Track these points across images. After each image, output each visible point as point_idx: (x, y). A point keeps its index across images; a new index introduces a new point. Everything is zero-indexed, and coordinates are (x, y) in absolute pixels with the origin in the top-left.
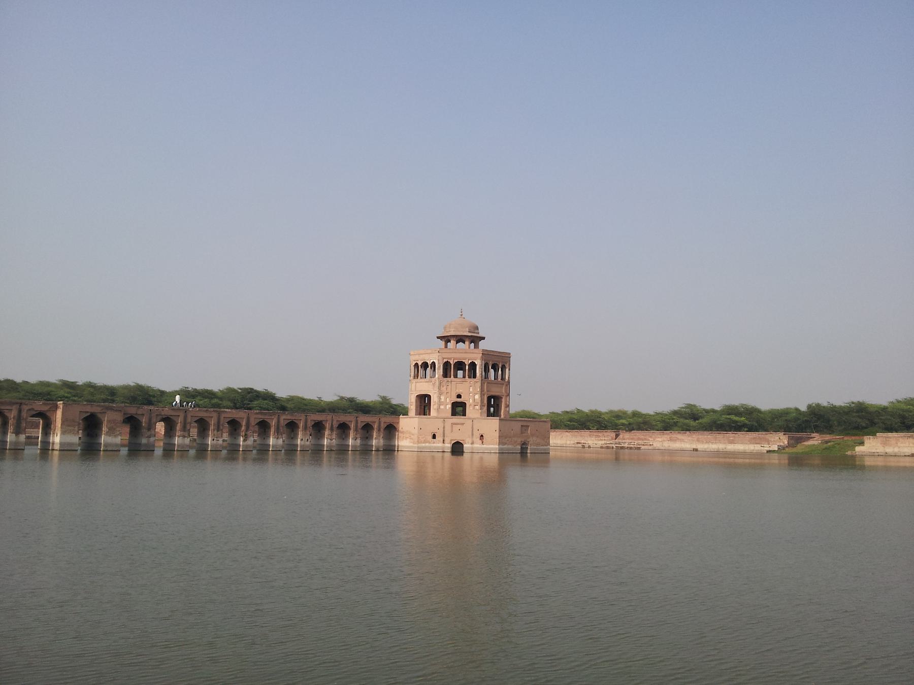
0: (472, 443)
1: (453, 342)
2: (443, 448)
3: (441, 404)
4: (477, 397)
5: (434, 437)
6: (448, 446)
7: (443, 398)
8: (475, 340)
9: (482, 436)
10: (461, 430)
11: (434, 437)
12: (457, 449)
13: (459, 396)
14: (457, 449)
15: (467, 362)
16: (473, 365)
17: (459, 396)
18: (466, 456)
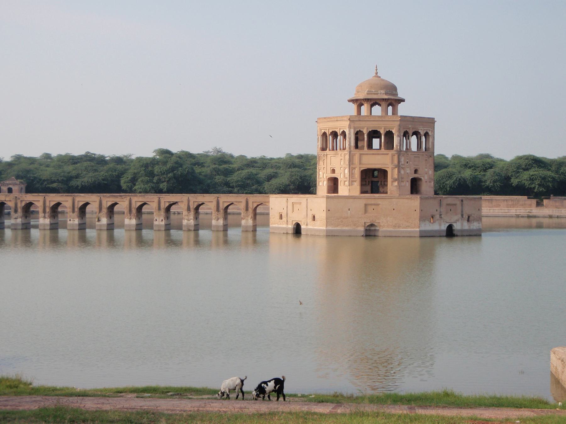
0: (307, 225)
1: (364, 109)
2: (287, 229)
4: (347, 171)
5: (281, 217)
6: (291, 226)
8: (393, 101)
9: (314, 217)
11: (281, 217)
12: (297, 230)
14: (297, 230)
17: (333, 171)
18: (303, 237)
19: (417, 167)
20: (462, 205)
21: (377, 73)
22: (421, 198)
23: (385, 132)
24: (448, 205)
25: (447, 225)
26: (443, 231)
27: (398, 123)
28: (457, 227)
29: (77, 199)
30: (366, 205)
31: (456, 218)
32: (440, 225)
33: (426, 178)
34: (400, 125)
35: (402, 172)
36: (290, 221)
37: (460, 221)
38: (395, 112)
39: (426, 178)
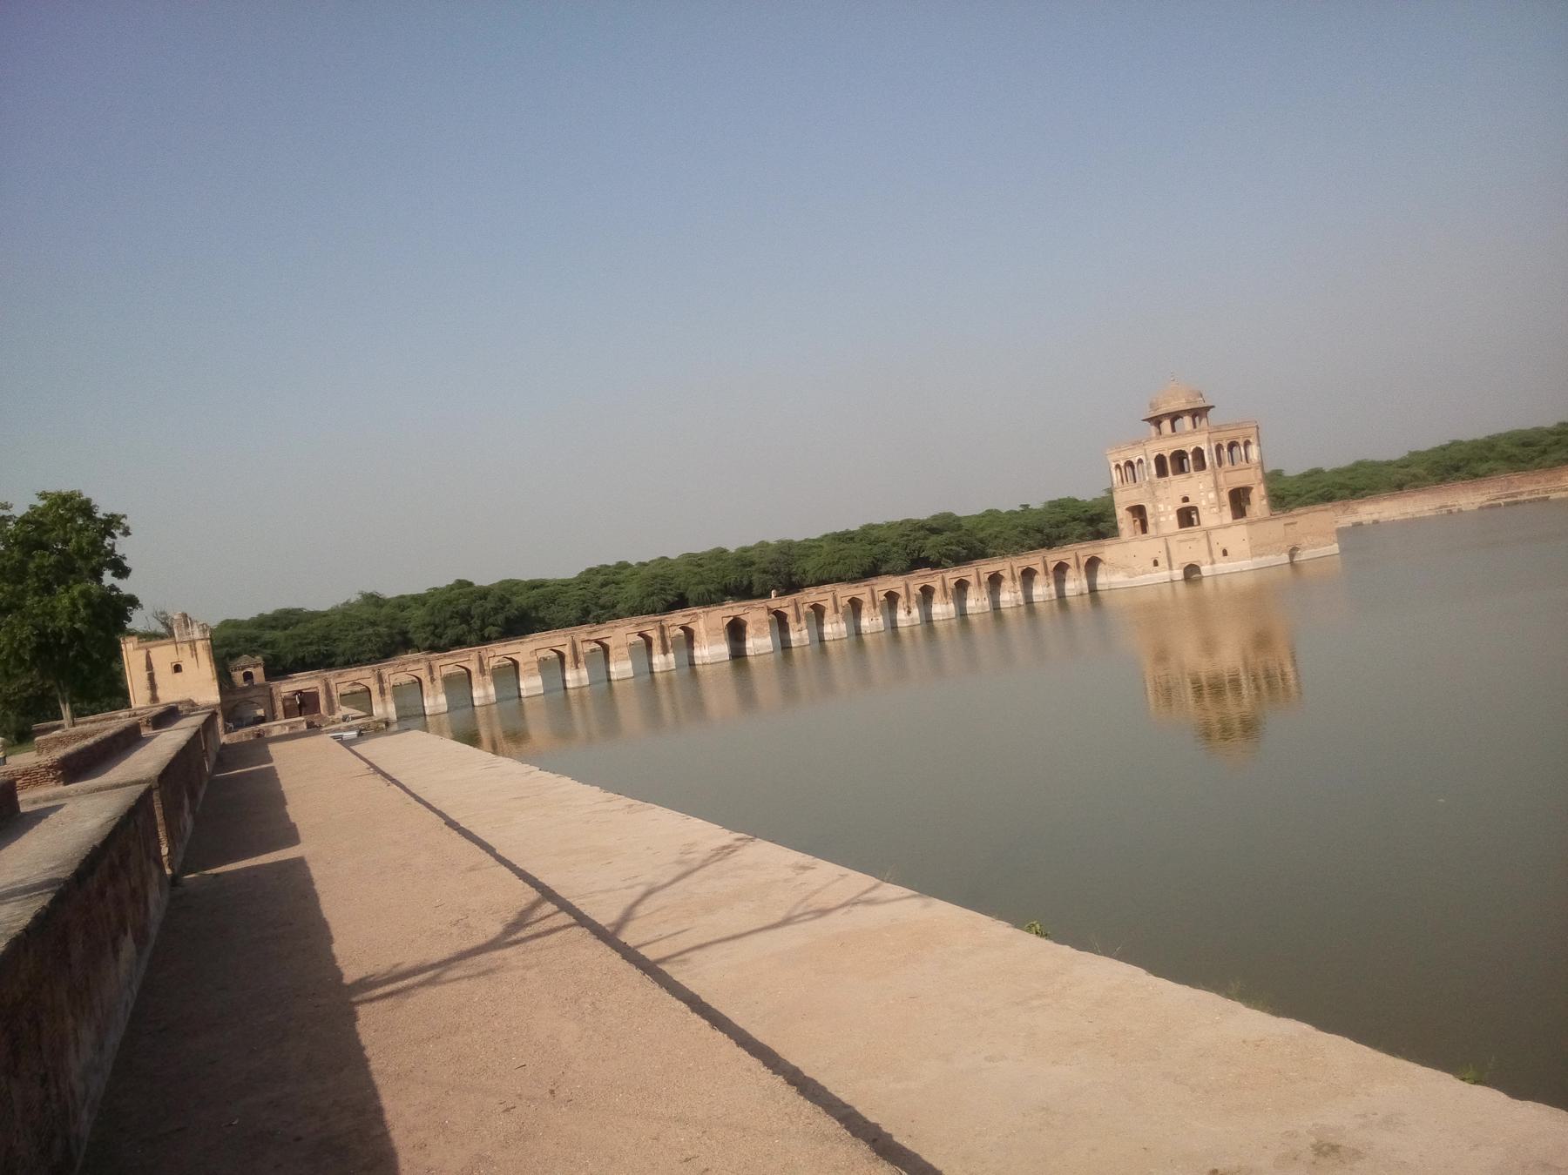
0: (1213, 563)
3: (1164, 514)
4: (1212, 495)
5: (1156, 563)
7: (1161, 506)
10: (1189, 548)
11: (1156, 563)
12: (1191, 572)
13: (1186, 499)
14: (1191, 572)
15: (1189, 450)
16: (1198, 453)
17: (1186, 499)
18: (1207, 583)
36: (1175, 565)
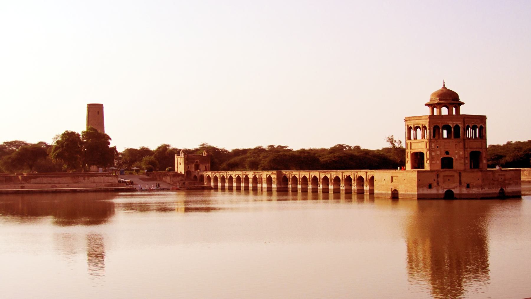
19: (446, 150)
20: (460, 176)
21: (444, 85)
22: (418, 171)
23: (452, 124)
24: (444, 176)
25: (445, 190)
26: (441, 194)
27: (428, 120)
28: (456, 191)
29: (311, 174)
30: (392, 177)
31: (454, 185)
32: (438, 190)
33: (457, 157)
34: (429, 122)
35: (433, 154)
37: (458, 187)
38: (458, 111)
39: (457, 157)
